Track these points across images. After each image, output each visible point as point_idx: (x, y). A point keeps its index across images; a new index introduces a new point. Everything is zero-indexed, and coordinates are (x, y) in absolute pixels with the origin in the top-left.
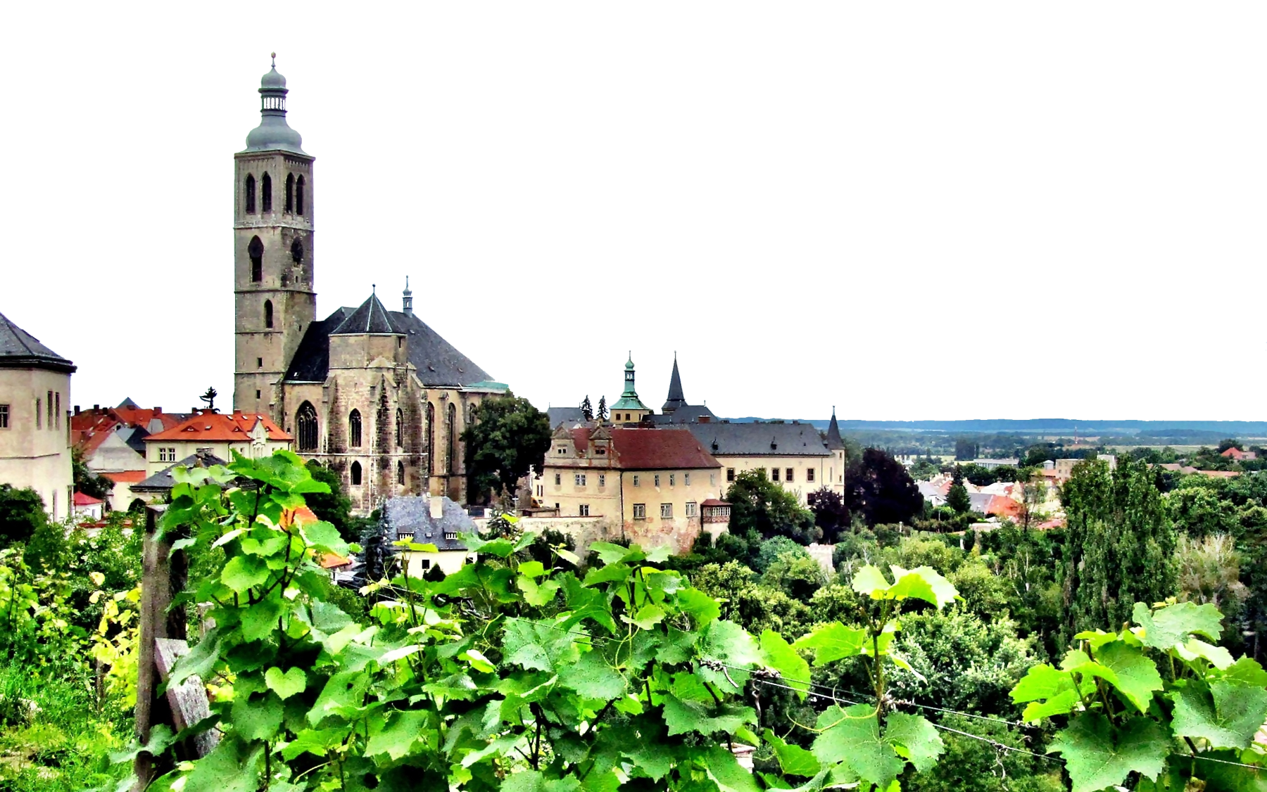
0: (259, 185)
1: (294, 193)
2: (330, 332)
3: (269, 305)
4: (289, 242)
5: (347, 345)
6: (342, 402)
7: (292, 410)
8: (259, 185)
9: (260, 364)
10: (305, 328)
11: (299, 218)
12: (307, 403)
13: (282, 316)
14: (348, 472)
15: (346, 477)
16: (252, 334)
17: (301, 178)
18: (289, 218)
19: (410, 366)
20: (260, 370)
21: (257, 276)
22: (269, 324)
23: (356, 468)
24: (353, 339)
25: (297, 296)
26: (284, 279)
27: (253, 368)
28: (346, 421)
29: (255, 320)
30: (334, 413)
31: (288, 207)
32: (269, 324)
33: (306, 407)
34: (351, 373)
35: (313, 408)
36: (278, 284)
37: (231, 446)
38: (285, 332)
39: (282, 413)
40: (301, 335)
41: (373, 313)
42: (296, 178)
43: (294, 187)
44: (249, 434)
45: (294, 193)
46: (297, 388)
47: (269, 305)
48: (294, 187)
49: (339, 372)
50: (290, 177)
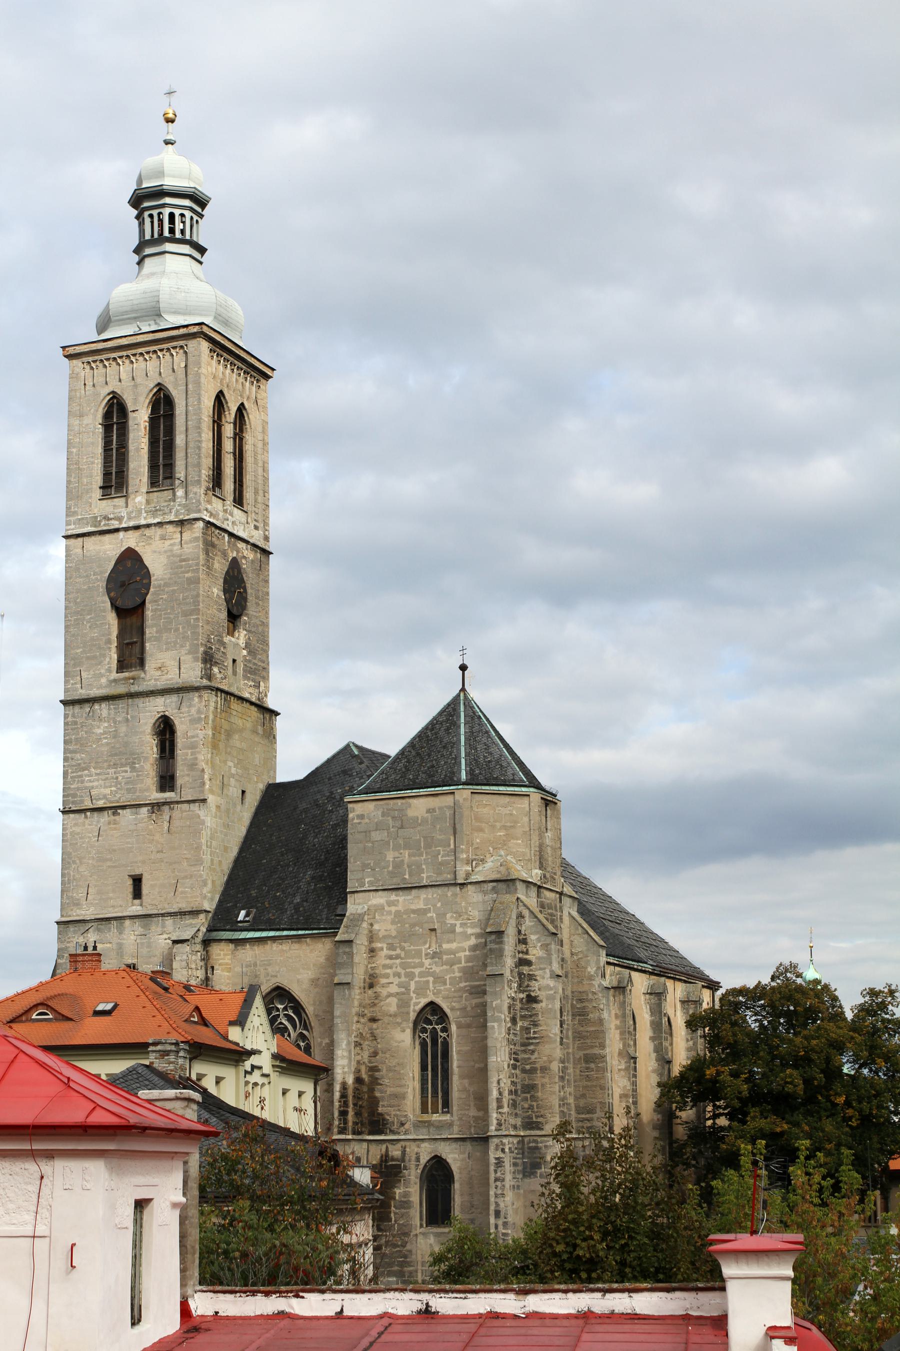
1: (228, 446)
2: (351, 792)
3: (165, 730)
4: (220, 566)
5: (403, 822)
6: (390, 987)
9: (137, 893)
13: (203, 756)
15: (405, 1204)
16: (115, 809)
17: (241, 409)
20: (136, 909)
21: (131, 655)
22: (167, 781)
23: (438, 1175)
24: (420, 806)
25: (235, 705)
26: (209, 659)
28: (403, 1041)
29: (126, 774)
31: (217, 481)
32: (167, 781)
34: (418, 901)
35: (298, 1007)
36: (193, 673)
38: (211, 799)
40: (246, 815)
41: (471, 737)
42: (232, 407)
43: (228, 430)
44: (235, 1034)
45: (228, 446)
46: (249, 953)
47: (165, 730)
48: (228, 430)
49: (379, 899)
50: (220, 400)
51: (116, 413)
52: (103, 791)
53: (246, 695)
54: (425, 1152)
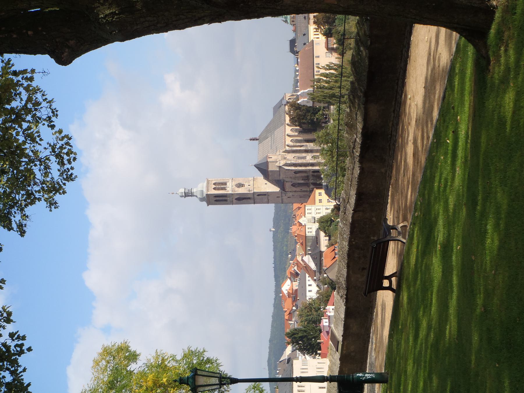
0: (218, 198)
1: (220, 186)
7: (294, 189)
8: (218, 198)
10: (266, 182)
11: (228, 184)
12: (292, 185)
14: (315, 174)
18: (228, 189)
19: (278, 153)
27: (280, 198)
30: (295, 178)
31: (224, 189)
33: (293, 185)
37: (307, 233)
39: (295, 191)
45: (220, 186)
50: (214, 189)
51: (216, 201)
52: (266, 200)
53: (252, 183)
54: (311, 173)
